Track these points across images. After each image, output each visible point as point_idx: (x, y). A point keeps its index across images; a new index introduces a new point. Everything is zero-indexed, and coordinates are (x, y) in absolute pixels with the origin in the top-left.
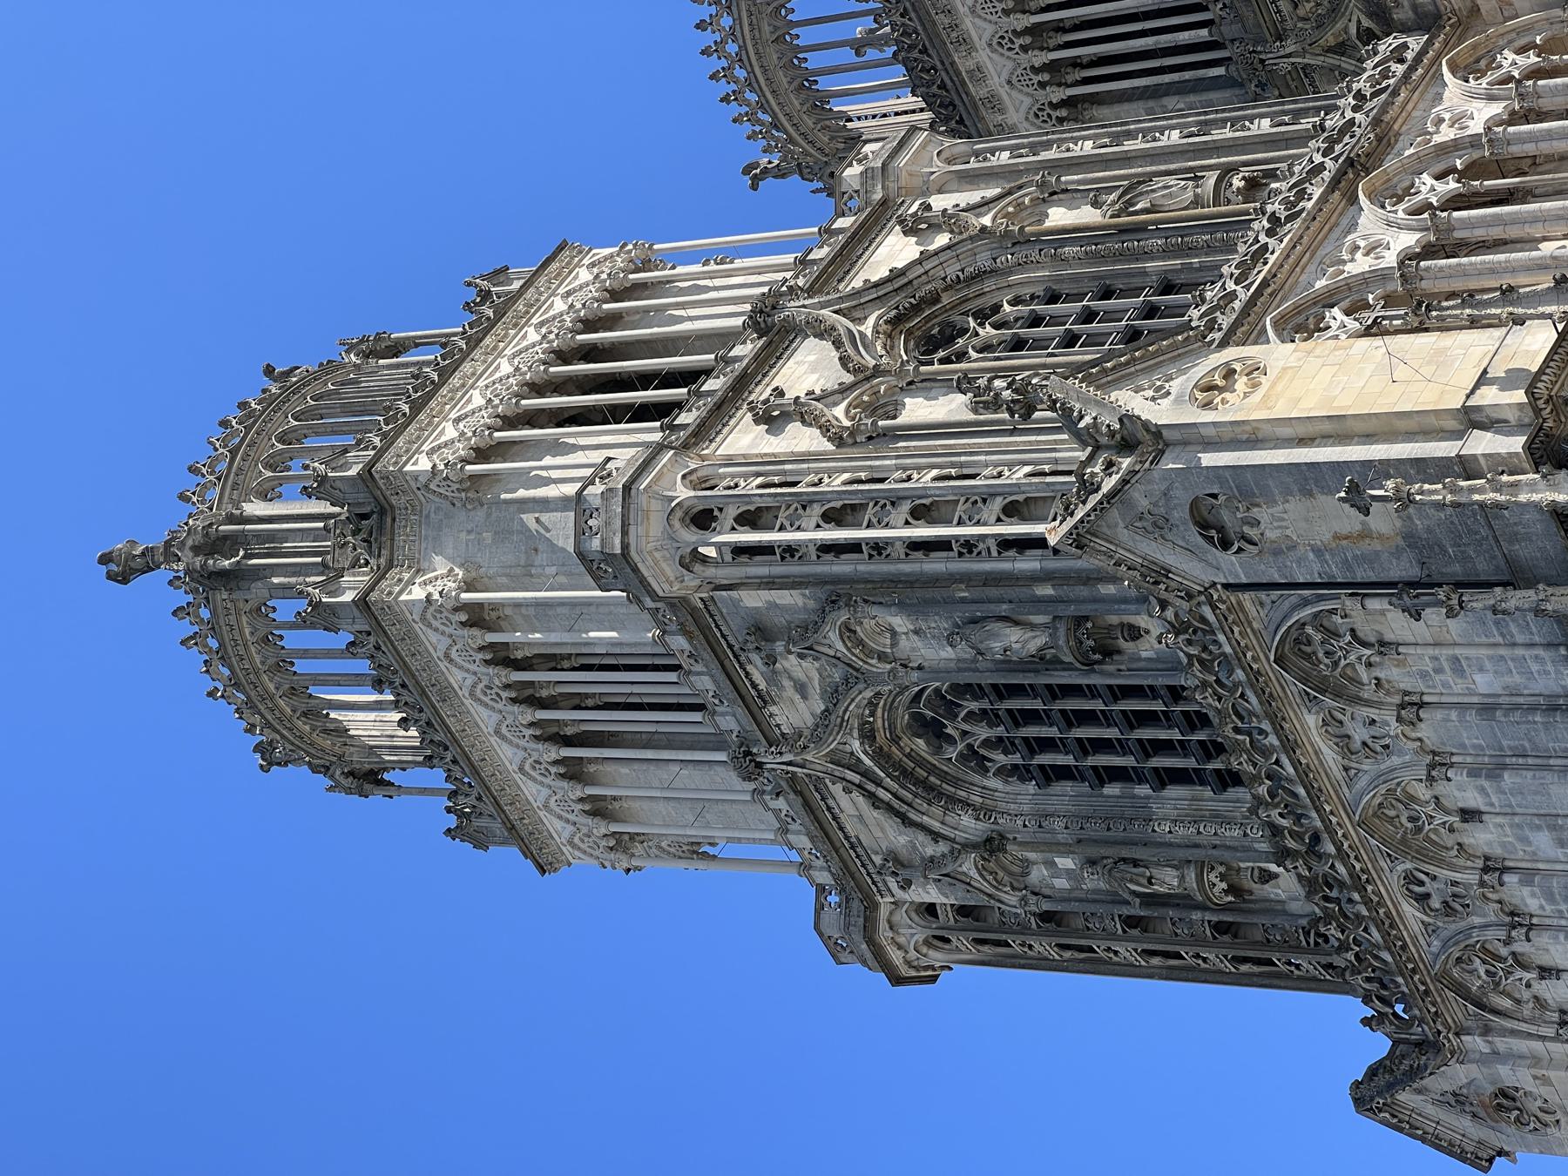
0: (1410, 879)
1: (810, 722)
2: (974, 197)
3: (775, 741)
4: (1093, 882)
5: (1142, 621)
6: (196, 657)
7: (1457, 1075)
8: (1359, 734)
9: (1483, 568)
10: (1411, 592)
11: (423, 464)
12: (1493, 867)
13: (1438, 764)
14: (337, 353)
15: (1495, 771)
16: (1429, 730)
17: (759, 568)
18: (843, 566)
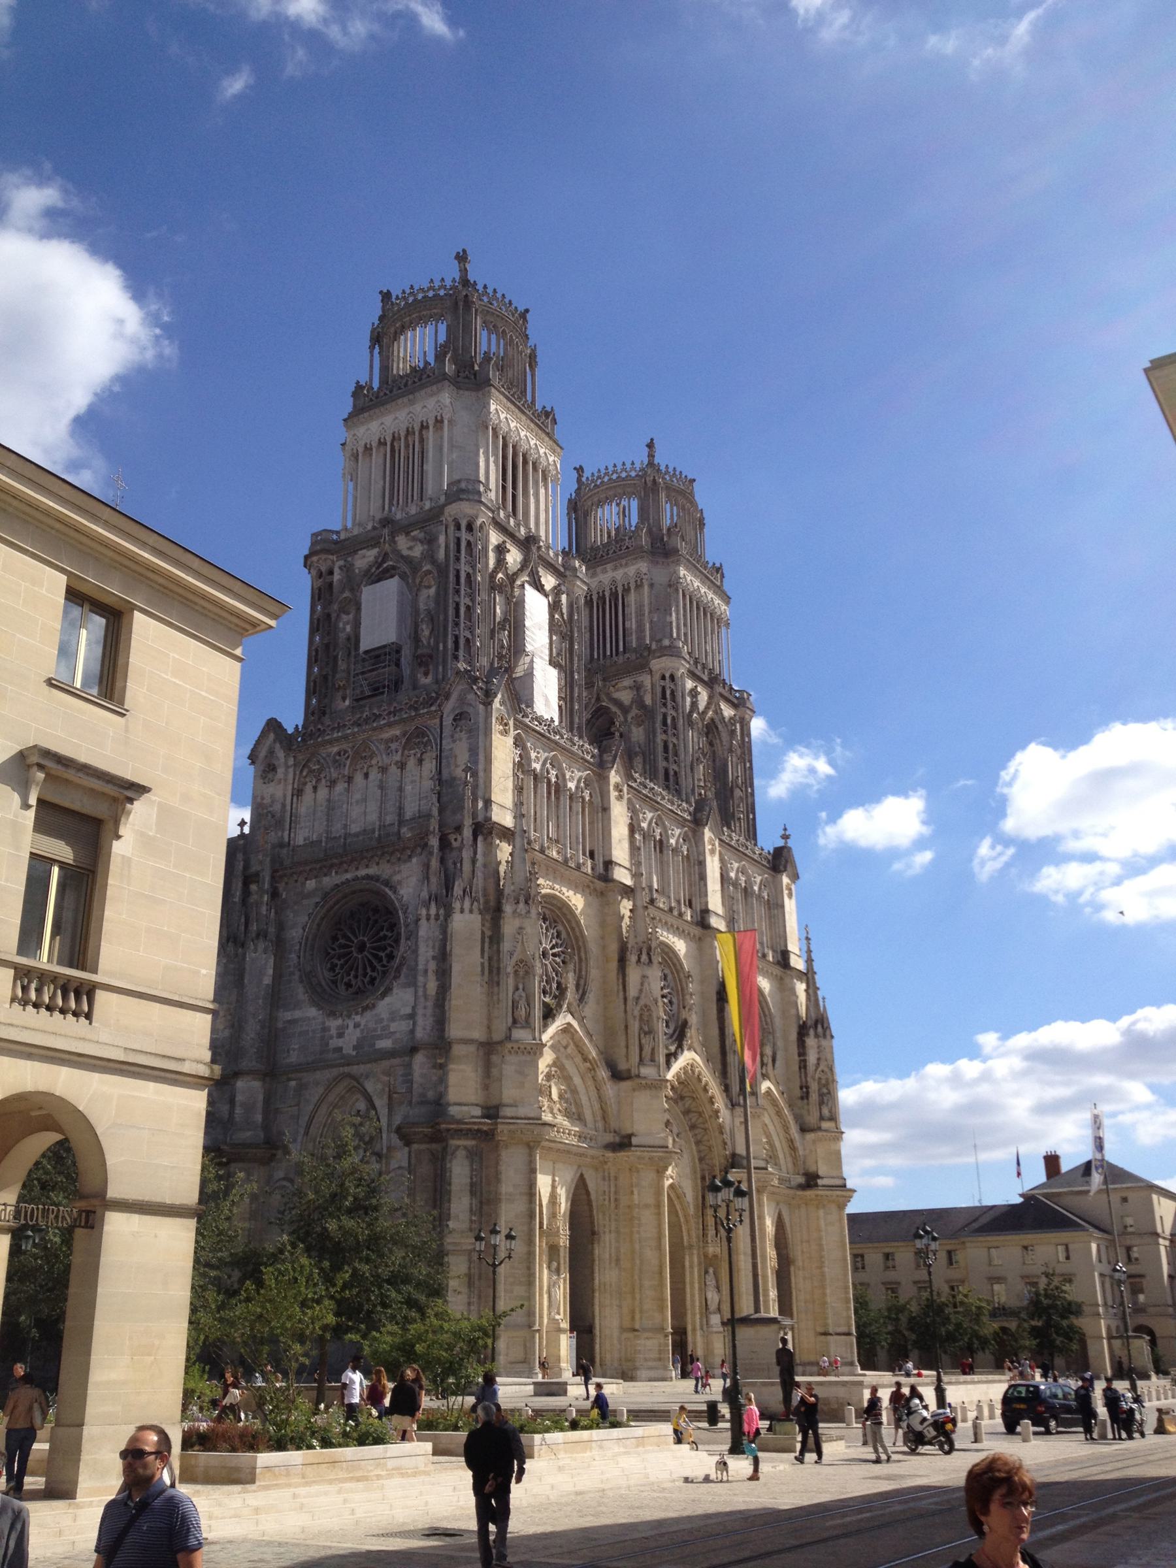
0: (346, 752)
1: (399, 548)
2: (564, 611)
3: (393, 535)
4: (342, 636)
5: (430, 677)
6: (426, 285)
7: (281, 754)
8: (393, 746)
9: (444, 799)
10: (439, 778)
11: (493, 407)
12: (350, 779)
13: (383, 770)
14: (531, 343)
15: (381, 787)
16: (394, 769)
17: (452, 546)
18: (452, 578)
